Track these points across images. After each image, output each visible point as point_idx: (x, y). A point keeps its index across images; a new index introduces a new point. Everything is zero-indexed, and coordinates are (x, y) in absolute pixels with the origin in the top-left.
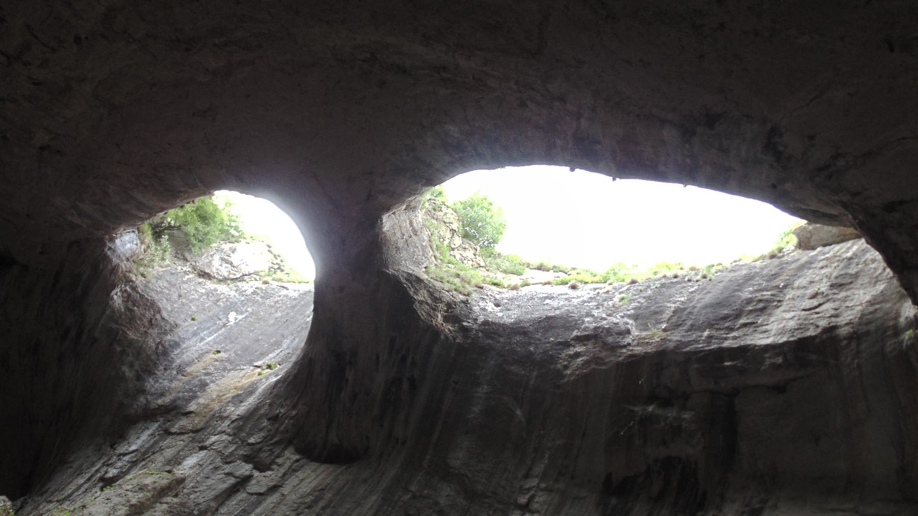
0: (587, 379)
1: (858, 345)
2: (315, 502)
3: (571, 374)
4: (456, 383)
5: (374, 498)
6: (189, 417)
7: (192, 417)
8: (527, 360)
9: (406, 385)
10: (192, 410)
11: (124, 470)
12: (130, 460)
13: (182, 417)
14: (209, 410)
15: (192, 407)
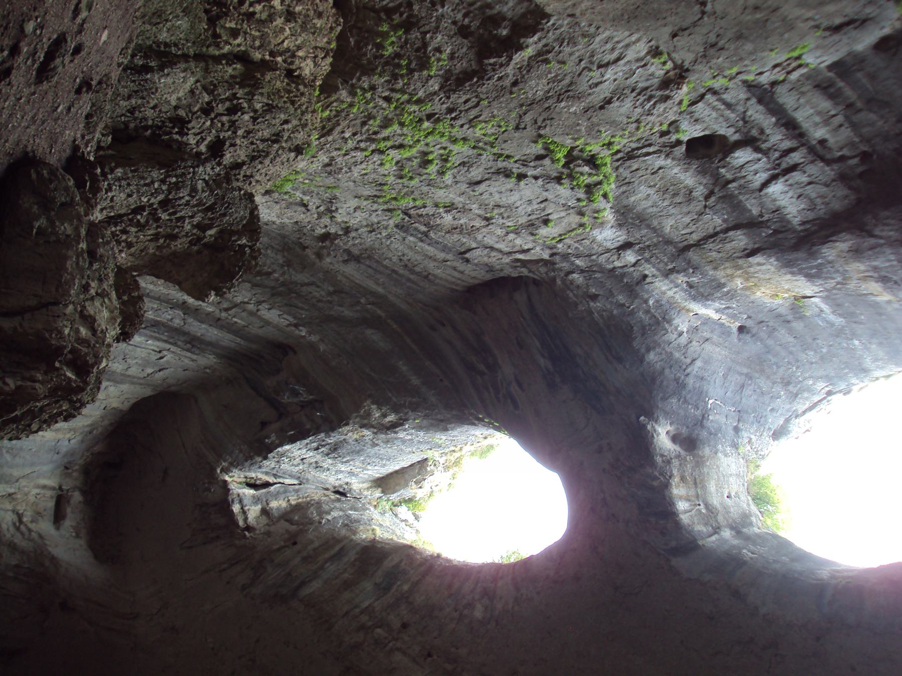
0: (357, 406)
1: (244, 455)
2: (412, 272)
3: (369, 406)
4: (441, 380)
5: (380, 290)
6: (743, 251)
7: (735, 253)
8: (415, 408)
9: (482, 367)
10: (750, 259)
11: (723, 171)
12: (742, 181)
13: (756, 246)
14: (723, 267)
15: (758, 259)
